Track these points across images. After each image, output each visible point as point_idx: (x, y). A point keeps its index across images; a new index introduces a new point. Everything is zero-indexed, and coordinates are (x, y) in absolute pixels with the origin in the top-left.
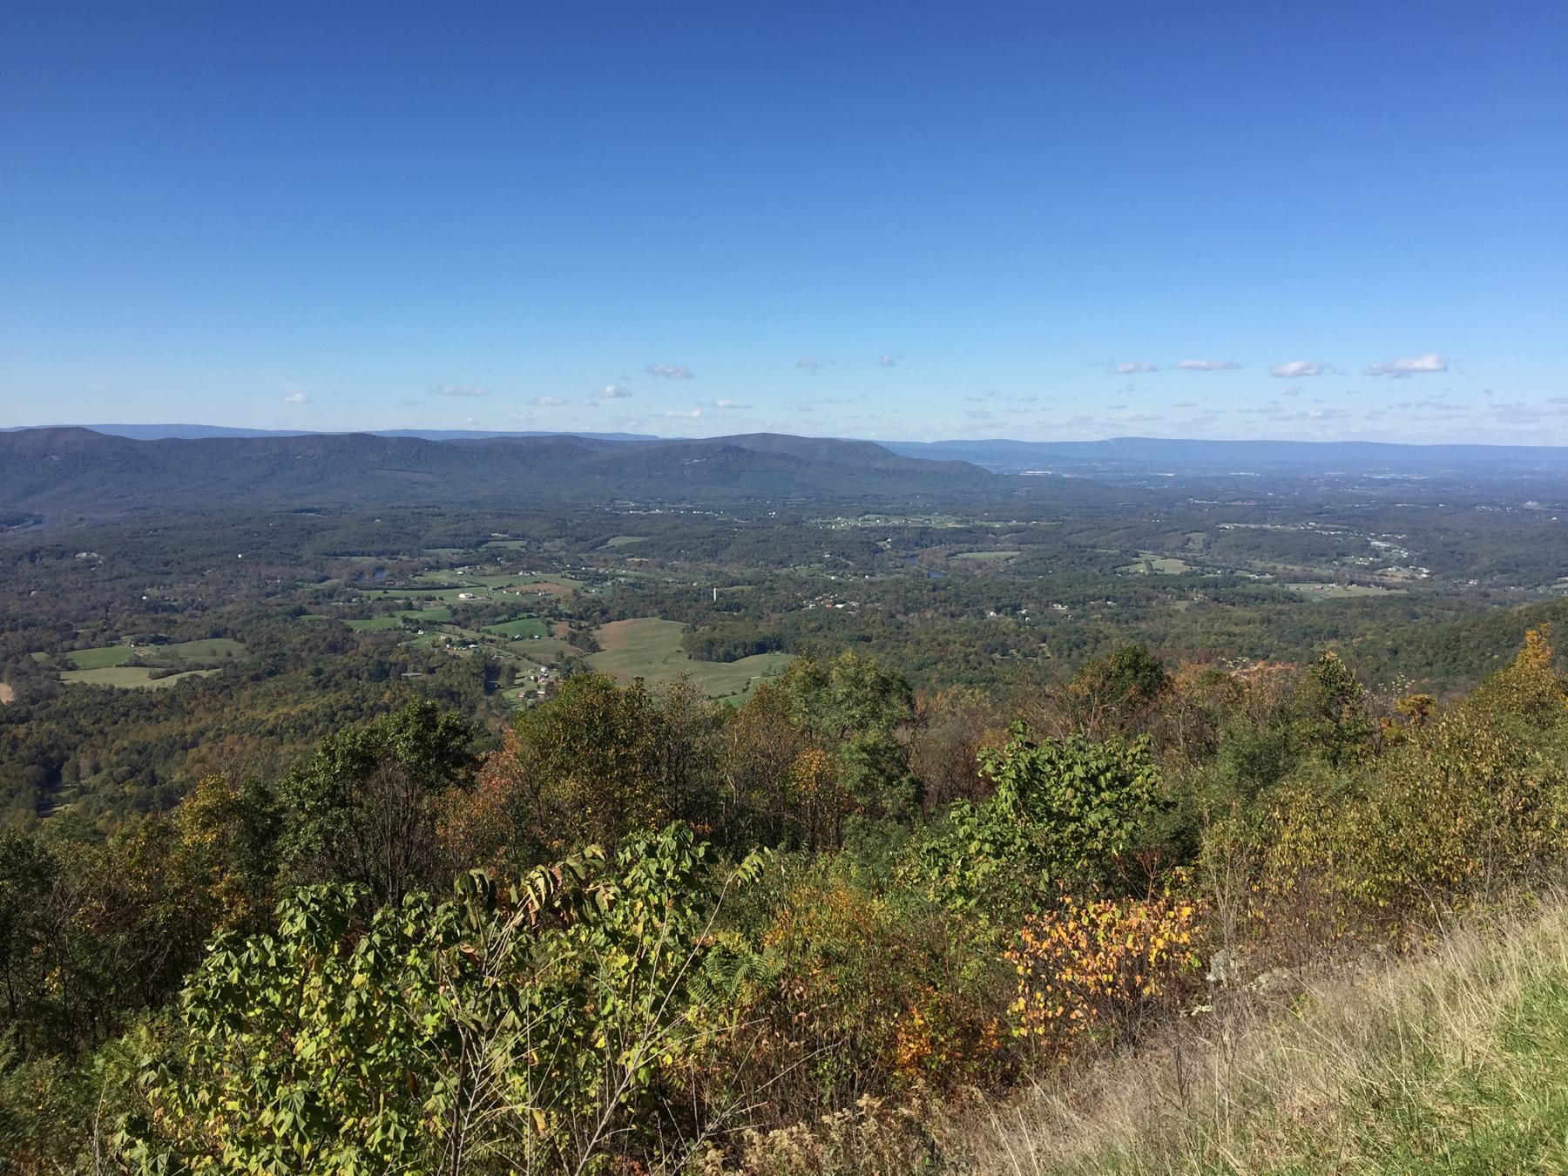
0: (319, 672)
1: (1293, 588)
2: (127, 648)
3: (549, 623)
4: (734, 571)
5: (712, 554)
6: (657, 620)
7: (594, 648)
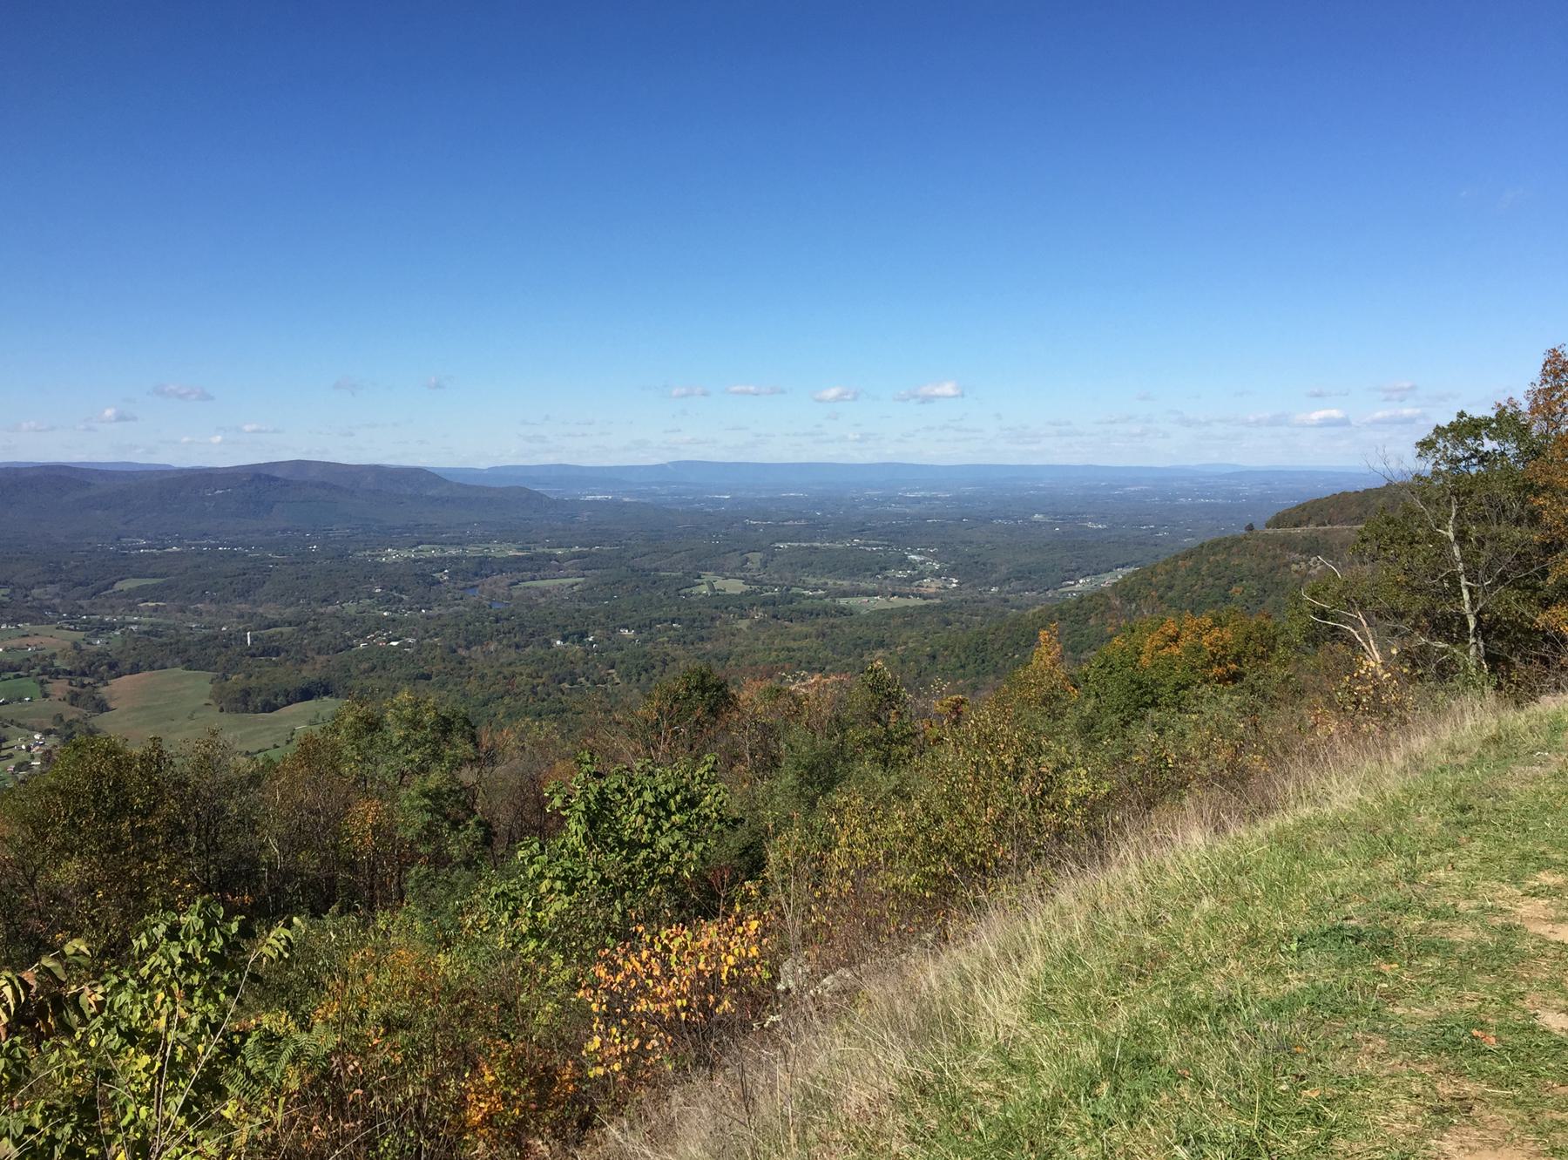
1: (843, 602)
3: (42, 682)
4: (271, 611)
5: (244, 594)
7: (102, 707)
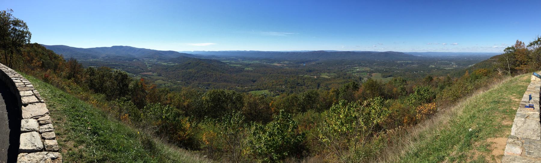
2: (326, 74)
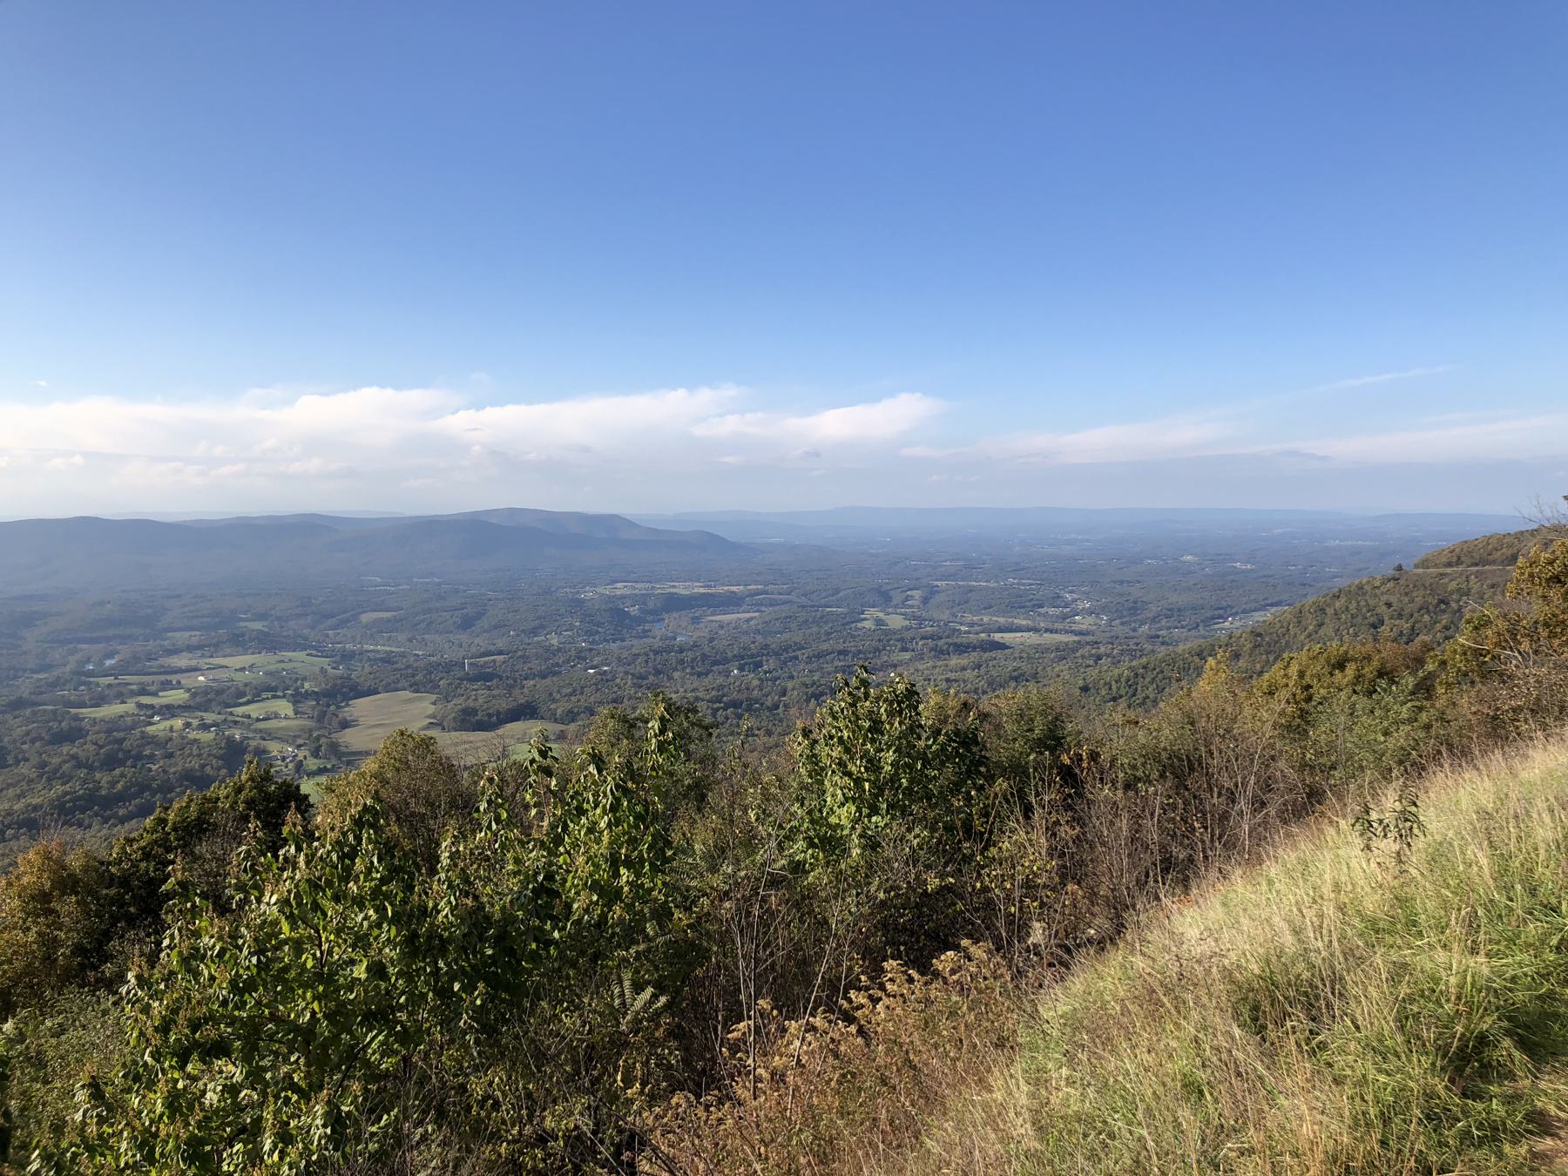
0: (42, 765)
1: (997, 637)
6: (407, 694)
